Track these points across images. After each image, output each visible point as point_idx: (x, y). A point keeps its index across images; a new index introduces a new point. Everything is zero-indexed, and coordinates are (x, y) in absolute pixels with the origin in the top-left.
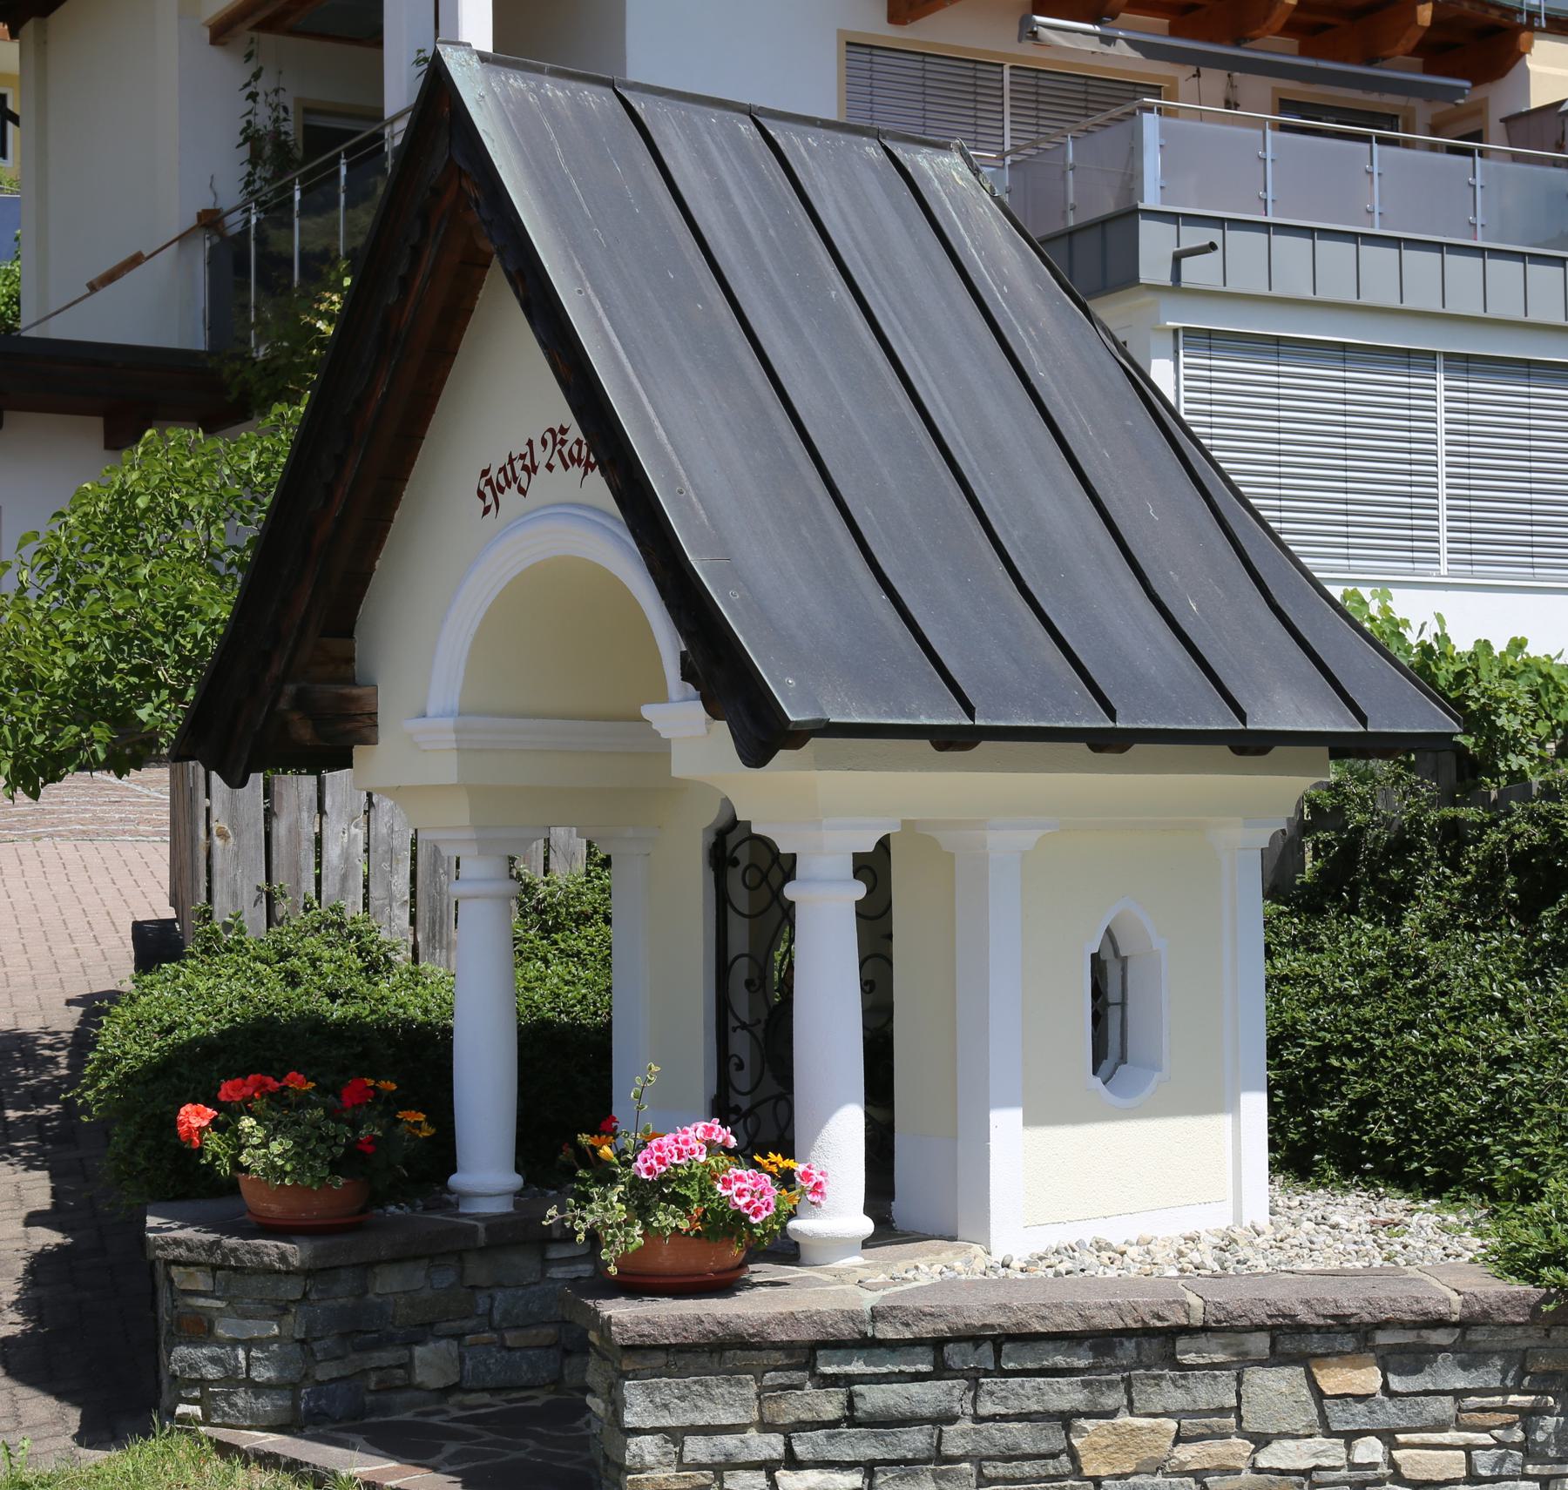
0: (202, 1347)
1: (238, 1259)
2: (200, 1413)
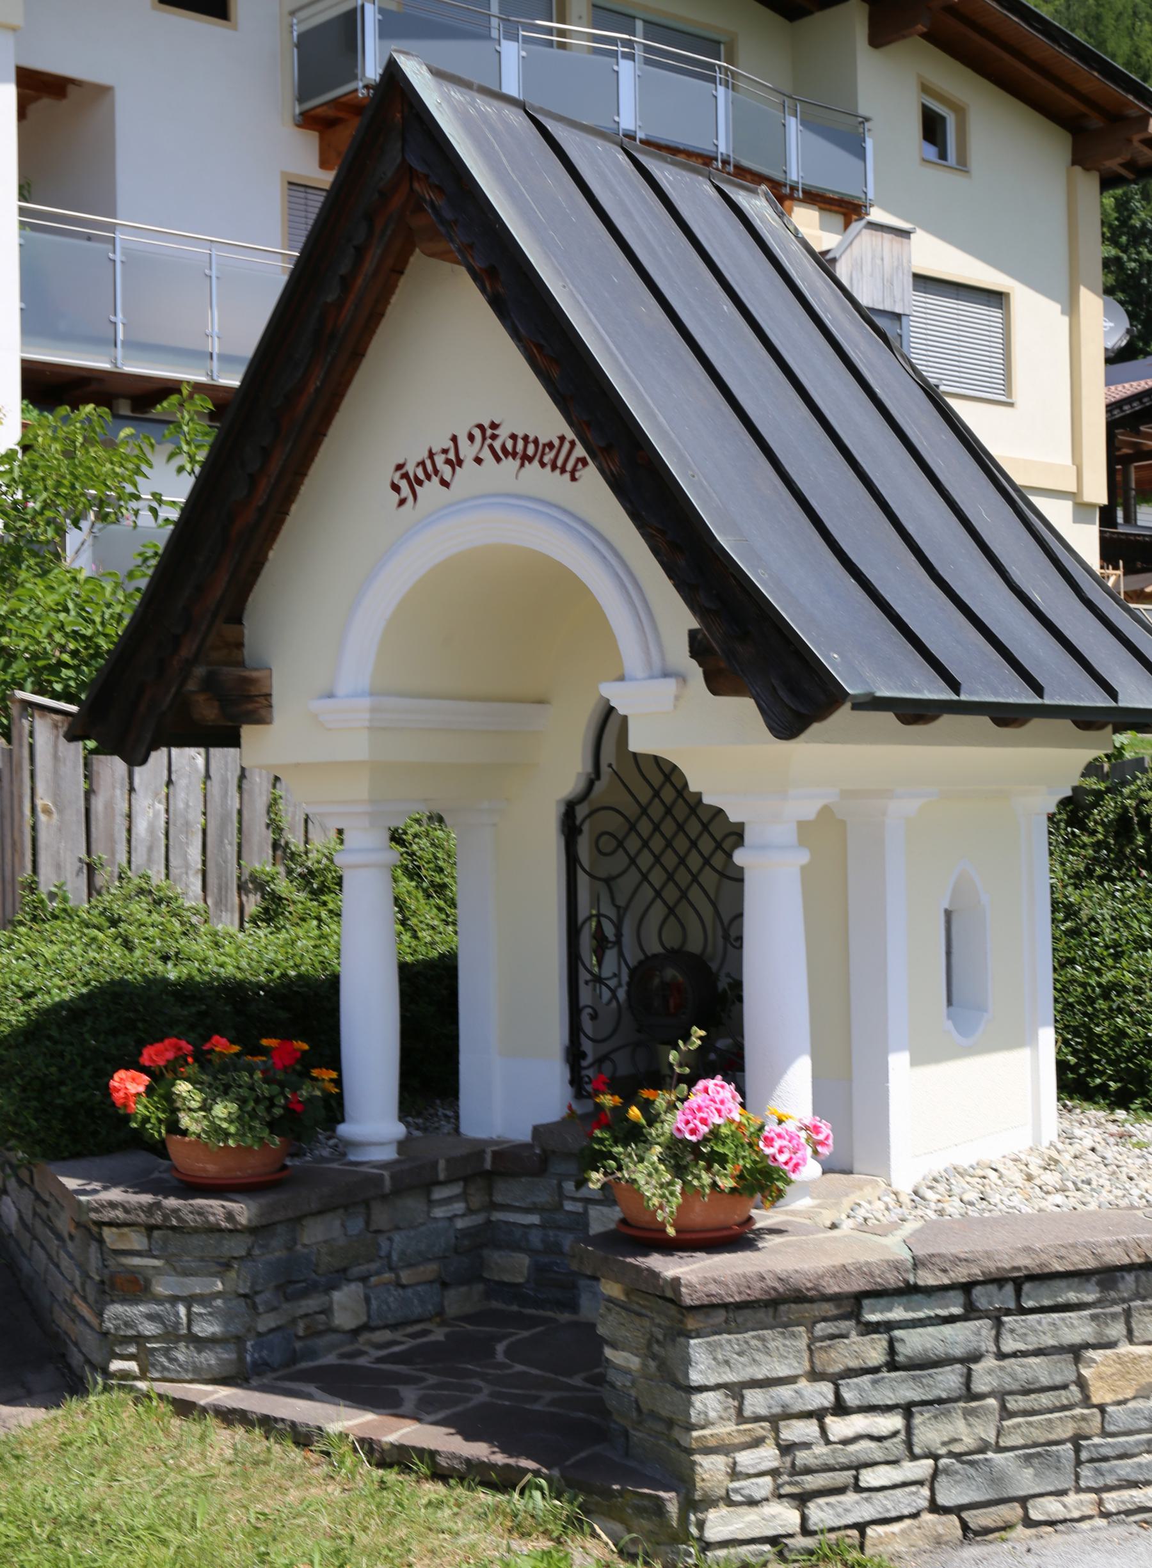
0: (137, 1304)
1: (179, 1219)
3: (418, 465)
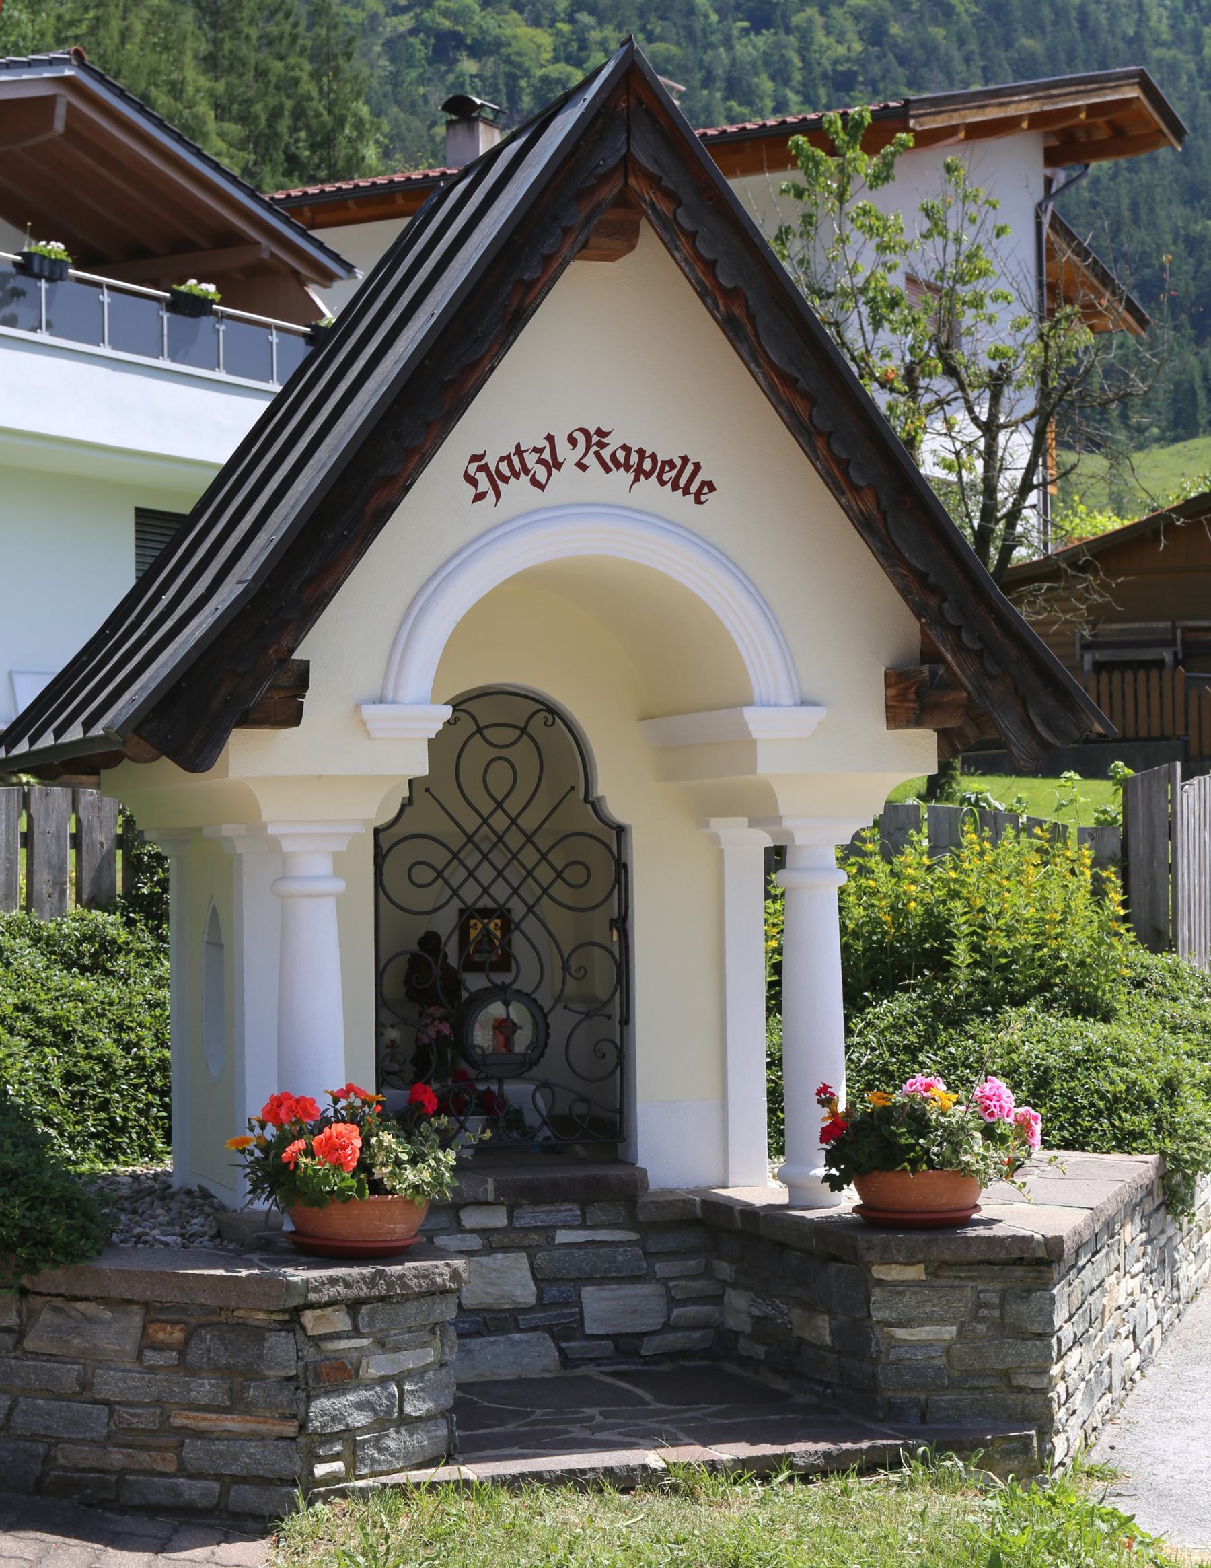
0: (345, 1394)
1: (404, 1286)
2: (218, 1490)
3: (501, 459)
